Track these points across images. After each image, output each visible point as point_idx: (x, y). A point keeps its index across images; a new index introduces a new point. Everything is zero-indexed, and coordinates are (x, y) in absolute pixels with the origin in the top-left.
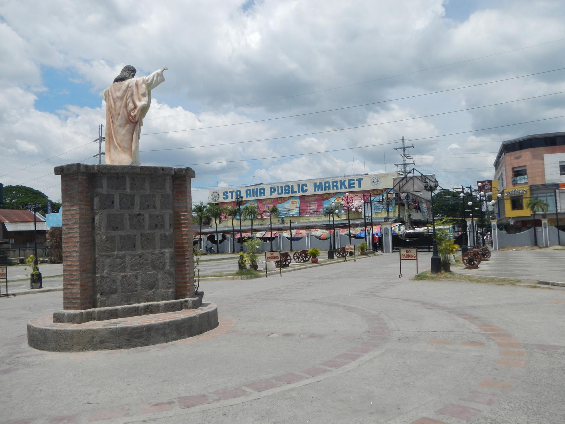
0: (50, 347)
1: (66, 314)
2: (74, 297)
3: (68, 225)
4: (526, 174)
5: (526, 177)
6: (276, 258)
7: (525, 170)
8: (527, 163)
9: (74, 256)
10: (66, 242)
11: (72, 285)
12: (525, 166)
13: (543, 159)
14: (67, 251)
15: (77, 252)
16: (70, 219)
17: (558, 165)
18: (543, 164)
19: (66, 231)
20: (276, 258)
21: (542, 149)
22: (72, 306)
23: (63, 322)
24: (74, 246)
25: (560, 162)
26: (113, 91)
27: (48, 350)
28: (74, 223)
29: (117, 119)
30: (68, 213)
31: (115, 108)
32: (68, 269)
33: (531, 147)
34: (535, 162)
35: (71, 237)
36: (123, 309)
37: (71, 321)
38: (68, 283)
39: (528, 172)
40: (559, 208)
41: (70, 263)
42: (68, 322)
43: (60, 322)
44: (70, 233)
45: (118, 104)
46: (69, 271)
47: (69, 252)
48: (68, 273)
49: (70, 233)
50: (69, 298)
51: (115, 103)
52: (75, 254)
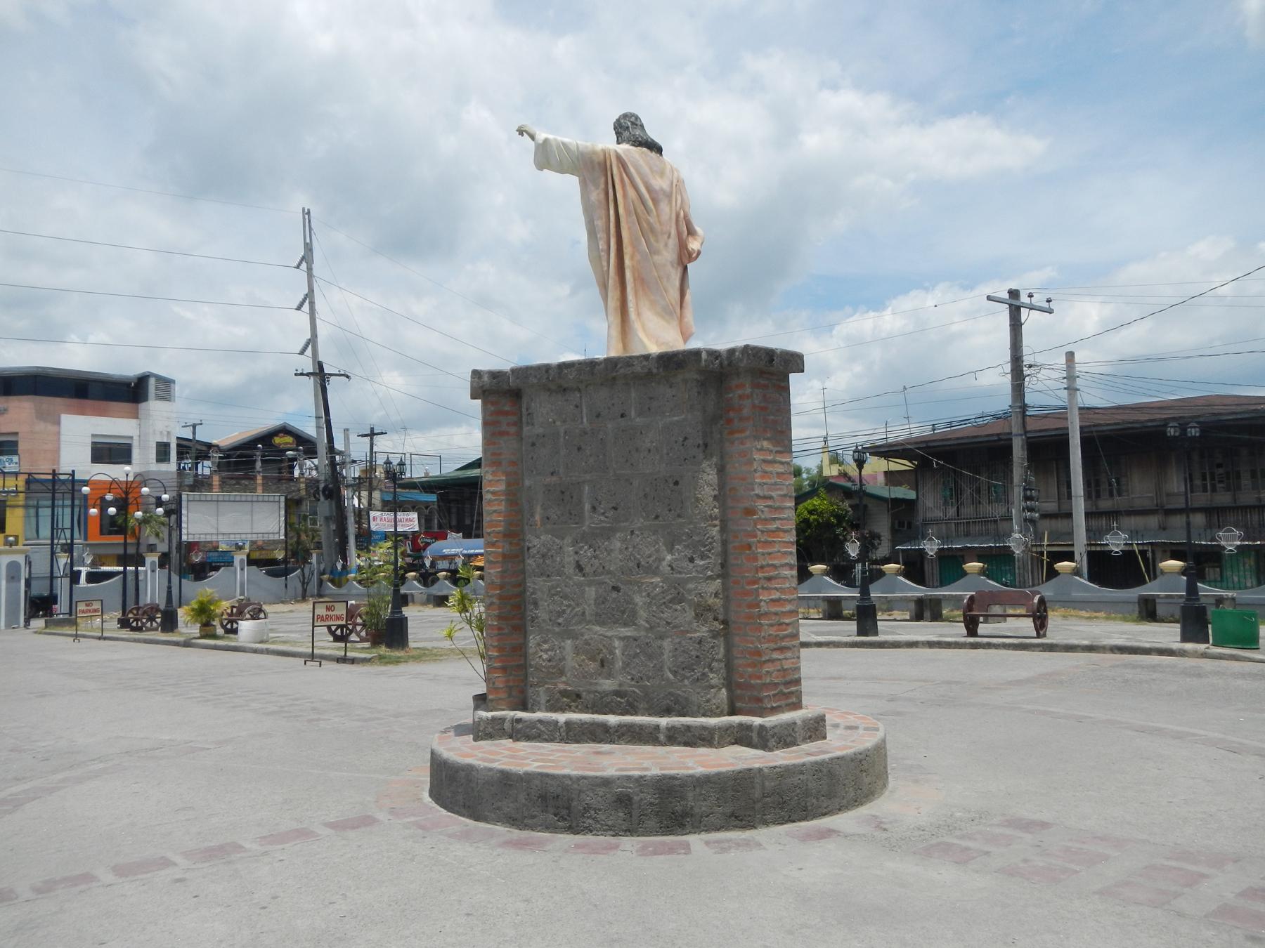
0: (845, 801)
1: (799, 722)
2: (788, 678)
3: (770, 498)
4: (15, 453)
5: (15, 459)
6: (338, 618)
7: (15, 444)
8: (22, 429)
9: (785, 578)
10: (766, 542)
11: (782, 649)
12: (16, 434)
13: (58, 423)
14: (768, 565)
15: (791, 567)
16: (775, 484)
17: (89, 441)
18: (59, 433)
19: (767, 515)
20: (338, 618)
21: (58, 400)
22: (783, 703)
23: (794, 744)
24: (785, 553)
25: (93, 436)
26: (646, 169)
27: (840, 810)
28: (785, 496)
29: (666, 245)
30: (769, 469)
31: (658, 216)
32: (773, 610)
33: (36, 393)
34: (41, 426)
35: (778, 529)
36: (620, 726)
37: (810, 737)
38: (773, 645)
39: (21, 447)
40: (184, 531)
41: (776, 595)
42: (805, 740)
43: (787, 745)
44: (774, 519)
45: (664, 206)
46: (776, 614)
47: (774, 566)
48: (774, 619)
49: (774, 519)
50: (776, 685)
51: (655, 201)
52: (787, 572)
